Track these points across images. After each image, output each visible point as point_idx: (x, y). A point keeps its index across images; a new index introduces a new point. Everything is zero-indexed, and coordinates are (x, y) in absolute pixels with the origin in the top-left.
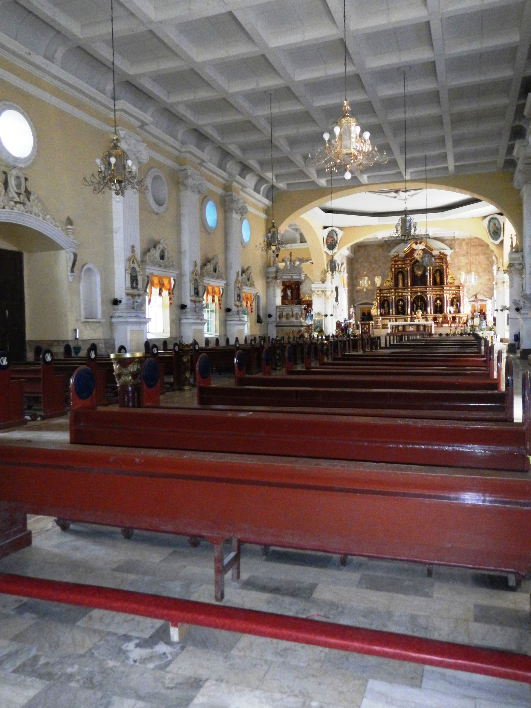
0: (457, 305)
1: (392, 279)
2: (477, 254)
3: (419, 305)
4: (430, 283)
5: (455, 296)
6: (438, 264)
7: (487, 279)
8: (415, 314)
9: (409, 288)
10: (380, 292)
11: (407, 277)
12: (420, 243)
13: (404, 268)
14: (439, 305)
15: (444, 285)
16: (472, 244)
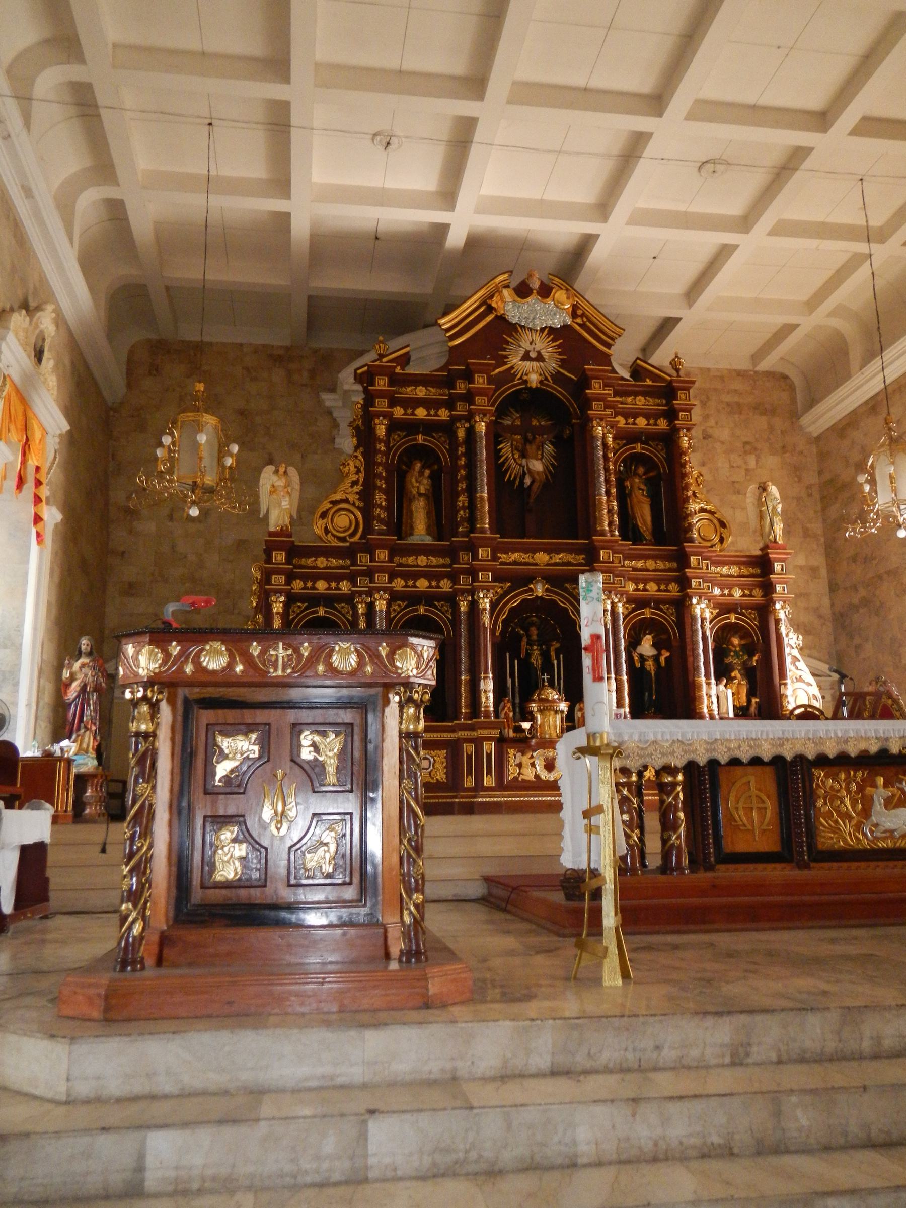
0: (749, 673)
1: (366, 495)
2: (749, 448)
3: (536, 660)
4: (610, 524)
5: (733, 618)
6: (642, 422)
7: (801, 568)
8: (531, 718)
9: (485, 543)
10: (289, 561)
11: (471, 479)
12: (545, 292)
13: (448, 428)
14: (650, 665)
15: (691, 540)
16: (727, 398)
